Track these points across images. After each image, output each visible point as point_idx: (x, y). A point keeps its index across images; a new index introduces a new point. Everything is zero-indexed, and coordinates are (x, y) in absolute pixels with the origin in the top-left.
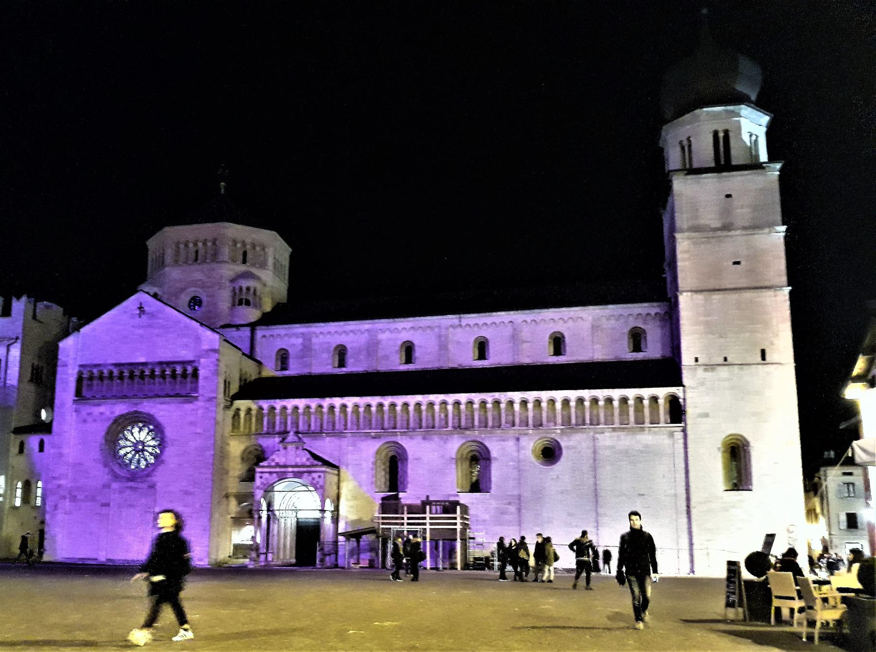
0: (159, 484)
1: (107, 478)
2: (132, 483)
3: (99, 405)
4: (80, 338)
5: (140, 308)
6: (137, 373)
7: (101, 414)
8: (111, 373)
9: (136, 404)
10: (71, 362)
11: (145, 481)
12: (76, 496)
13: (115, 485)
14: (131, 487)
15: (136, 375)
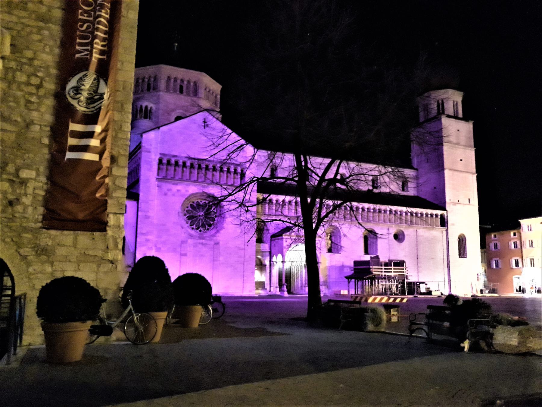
0: (221, 243)
1: (183, 236)
2: (203, 240)
3: (177, 184)
4: (160, 133)
5: (205, 122)
6: (204, 166)
7: (178, 191)
8: (184, 163)
9: (204, 187)
10: (153, 150)
11: (211, 240)
12: (160, 248)
13: (190, 241)
14: (202, 243)
15: (204, 168)
